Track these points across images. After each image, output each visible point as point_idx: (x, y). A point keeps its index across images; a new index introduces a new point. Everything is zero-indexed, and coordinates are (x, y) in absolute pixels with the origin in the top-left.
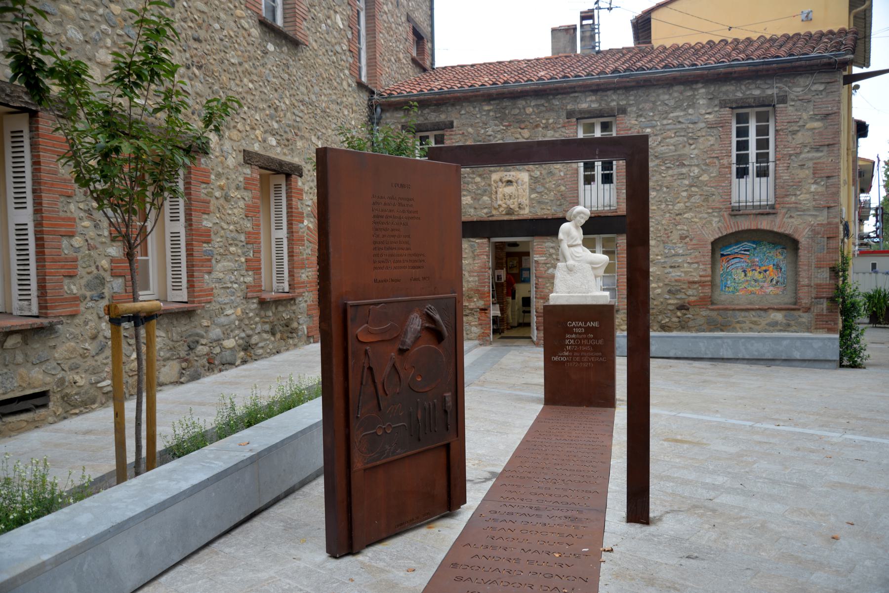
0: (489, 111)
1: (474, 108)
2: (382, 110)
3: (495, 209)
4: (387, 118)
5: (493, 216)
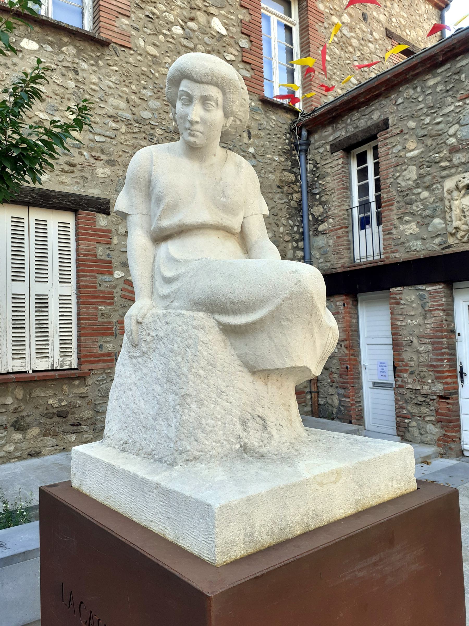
0: (437, 84)
1: (415, 89)
2: (310, 133)
3: (452, 235)
4: (316, 141)
5: (449, 247)
